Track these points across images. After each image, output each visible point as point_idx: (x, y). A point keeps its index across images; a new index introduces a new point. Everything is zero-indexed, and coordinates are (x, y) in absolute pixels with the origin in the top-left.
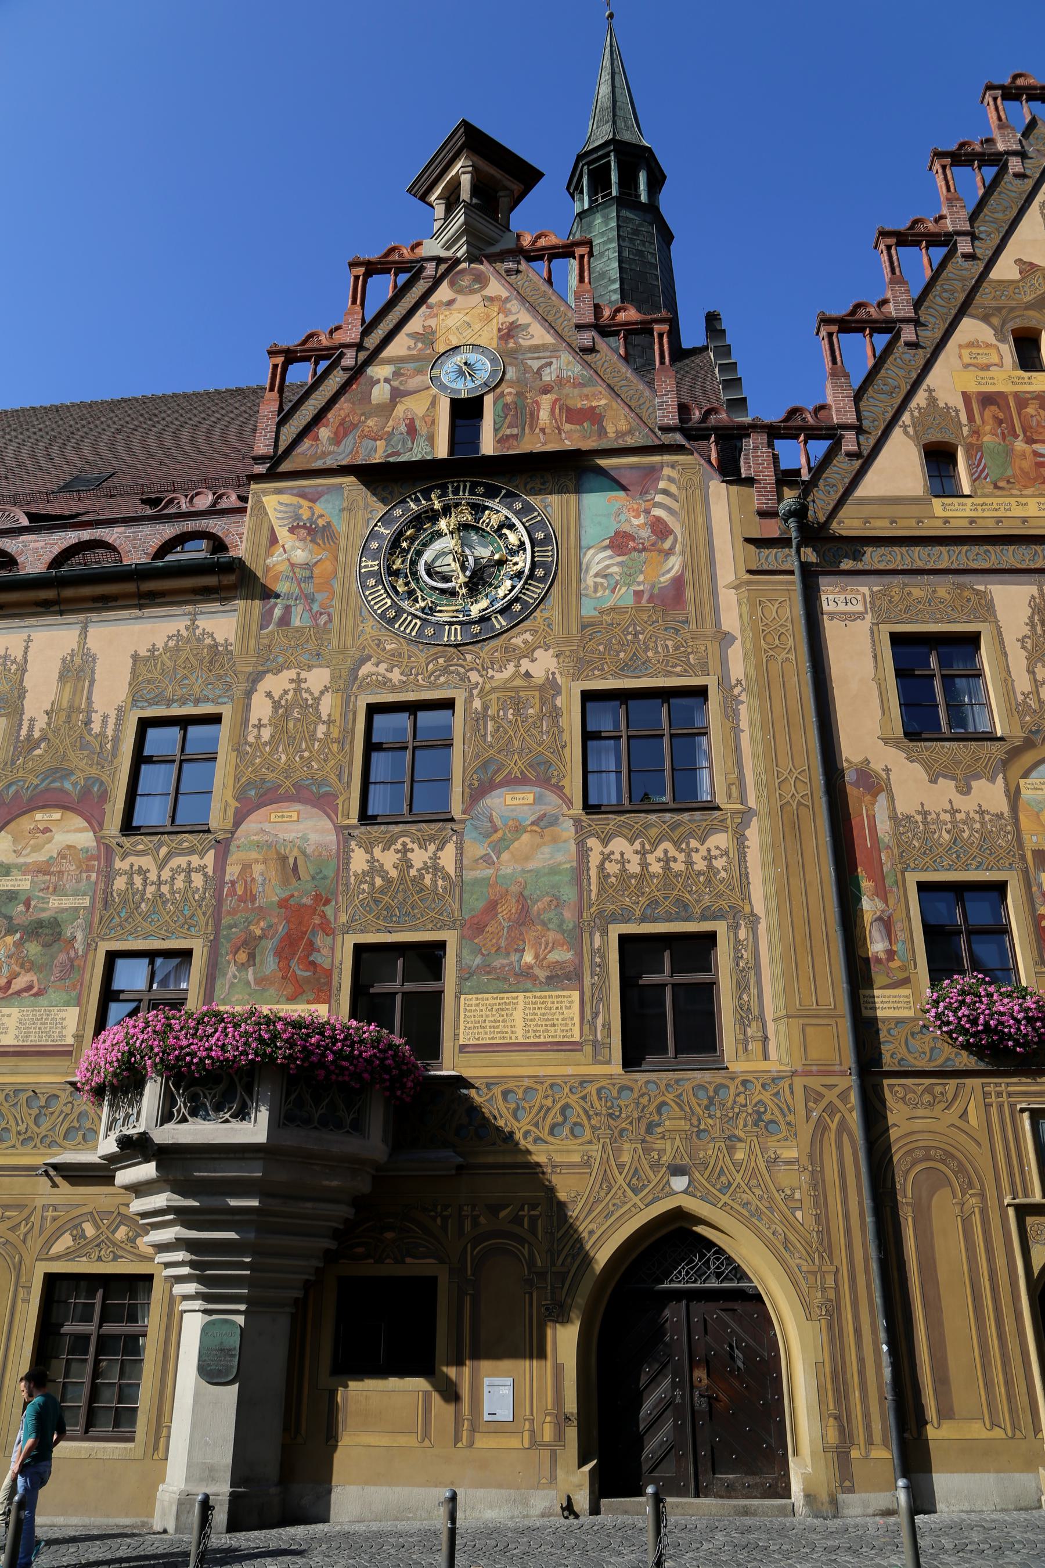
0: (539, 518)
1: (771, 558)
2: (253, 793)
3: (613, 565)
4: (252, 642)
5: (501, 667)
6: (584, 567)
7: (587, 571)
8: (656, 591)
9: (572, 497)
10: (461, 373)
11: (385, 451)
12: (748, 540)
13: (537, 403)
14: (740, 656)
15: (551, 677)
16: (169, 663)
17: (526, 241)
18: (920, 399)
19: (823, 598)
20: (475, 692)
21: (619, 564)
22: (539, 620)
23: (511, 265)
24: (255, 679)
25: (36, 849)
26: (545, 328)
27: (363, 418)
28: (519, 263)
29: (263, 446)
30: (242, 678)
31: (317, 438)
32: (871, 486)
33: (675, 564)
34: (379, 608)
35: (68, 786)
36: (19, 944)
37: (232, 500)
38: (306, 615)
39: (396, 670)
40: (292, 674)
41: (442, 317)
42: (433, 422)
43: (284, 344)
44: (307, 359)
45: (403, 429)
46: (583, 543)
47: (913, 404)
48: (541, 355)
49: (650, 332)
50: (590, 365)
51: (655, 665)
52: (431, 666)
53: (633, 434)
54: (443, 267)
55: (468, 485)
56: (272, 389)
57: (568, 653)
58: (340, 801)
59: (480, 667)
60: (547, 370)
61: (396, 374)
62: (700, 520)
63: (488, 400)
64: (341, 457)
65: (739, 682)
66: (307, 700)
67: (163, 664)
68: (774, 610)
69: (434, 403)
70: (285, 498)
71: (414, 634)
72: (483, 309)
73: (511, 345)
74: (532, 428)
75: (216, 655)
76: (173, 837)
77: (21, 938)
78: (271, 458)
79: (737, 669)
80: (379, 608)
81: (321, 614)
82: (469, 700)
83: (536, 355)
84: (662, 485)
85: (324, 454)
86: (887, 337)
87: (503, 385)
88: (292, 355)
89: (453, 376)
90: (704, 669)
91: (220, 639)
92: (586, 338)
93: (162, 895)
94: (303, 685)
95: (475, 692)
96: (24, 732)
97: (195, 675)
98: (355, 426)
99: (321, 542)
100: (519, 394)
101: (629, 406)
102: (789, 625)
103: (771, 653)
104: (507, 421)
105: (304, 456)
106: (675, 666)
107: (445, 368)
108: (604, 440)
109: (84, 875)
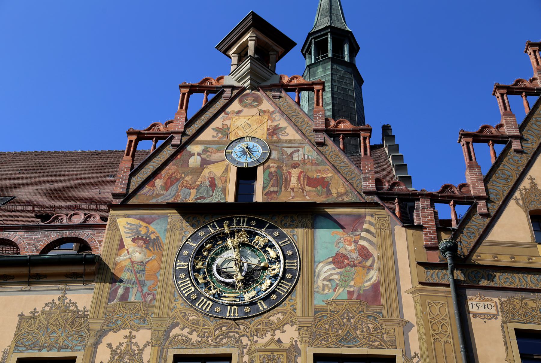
0: (289, 242)
1: (435, 276)
3: (335, 274)
4: (102, 310)
5: (262, 335)
6: (316, 274)
7: (318, 276)
8: (362, 292)
9: (310, 231)
10: (244, 153)
11: (195, 196)
12: (419, 264)
13: (289, 173)
14: (417, 337)
15: (294, 343)
16: (44, 322)
17: (285, 80)
18: (526, 183)
19: (469, 303)
20: (245, 351)
21: (339, 273)
22: (288, 306)
23: (276, 93)
24: (102, 334)
26: (295, 130)
27: (183, 175)
28: (281, 92)
29: (120, 188)
30: (92, 333)
31: (154, 186)
32: (498, 234)
33: (374, 276)
34: (186, 293)
37: (96, 219)
38: (139, 294)
39: (194, 333)
40: (126, 332)
41: (234, 120)
42: (226, 181)
43: (137, 129)
44: (150, 138)
45: (208, 183)
46: (316, 259)
47: (521, 186)
48: (293, 145)
49: (359, 136)
50: (322, 153)
51: (361, 340)
52: (217, 332)
53: (348, 195)
54: (235, 92)
55: (246, 219)
56: (128, 155)
57: (305, 329)
59: (249, 334)
60: (296, 155)
61: (205, 151)
62: (389, 249)
63: (260, 170)
64: (168, 198)
65: (416, 355)
66: (135, 350)
67: (40, 322)
68: (438, 308)
69: (227, 169)
70: (131, 220)
71: (207, 310)
72: (259, 117)
73: (275, 138)
74: (286, 188)
75: (77, 317)
78: (124, 195)
79: (415, 347)
80: (186, 293)
81: (149, 294)
82: (241, 356)
83: (290, 145)
84: (365, 226)
85: (158, 195)
86: (503, 146)
87: (270, 161)
88: (141, 136)
89: (239, 154)
90: (393, 344)
91: (80, 307)
92: (320, 137)
94: (133, 340)
95: (245, 351)
97: (61, 330)
98: (178, 180)
99: (152, 249)
100: (279, 167)
101: (346, 178)
102: (448, 319)
103: (437, 337)
104: (271, 183)
105: (146, 195)
106: (374, 341)
107: (235, 149)
108: (330, 198)
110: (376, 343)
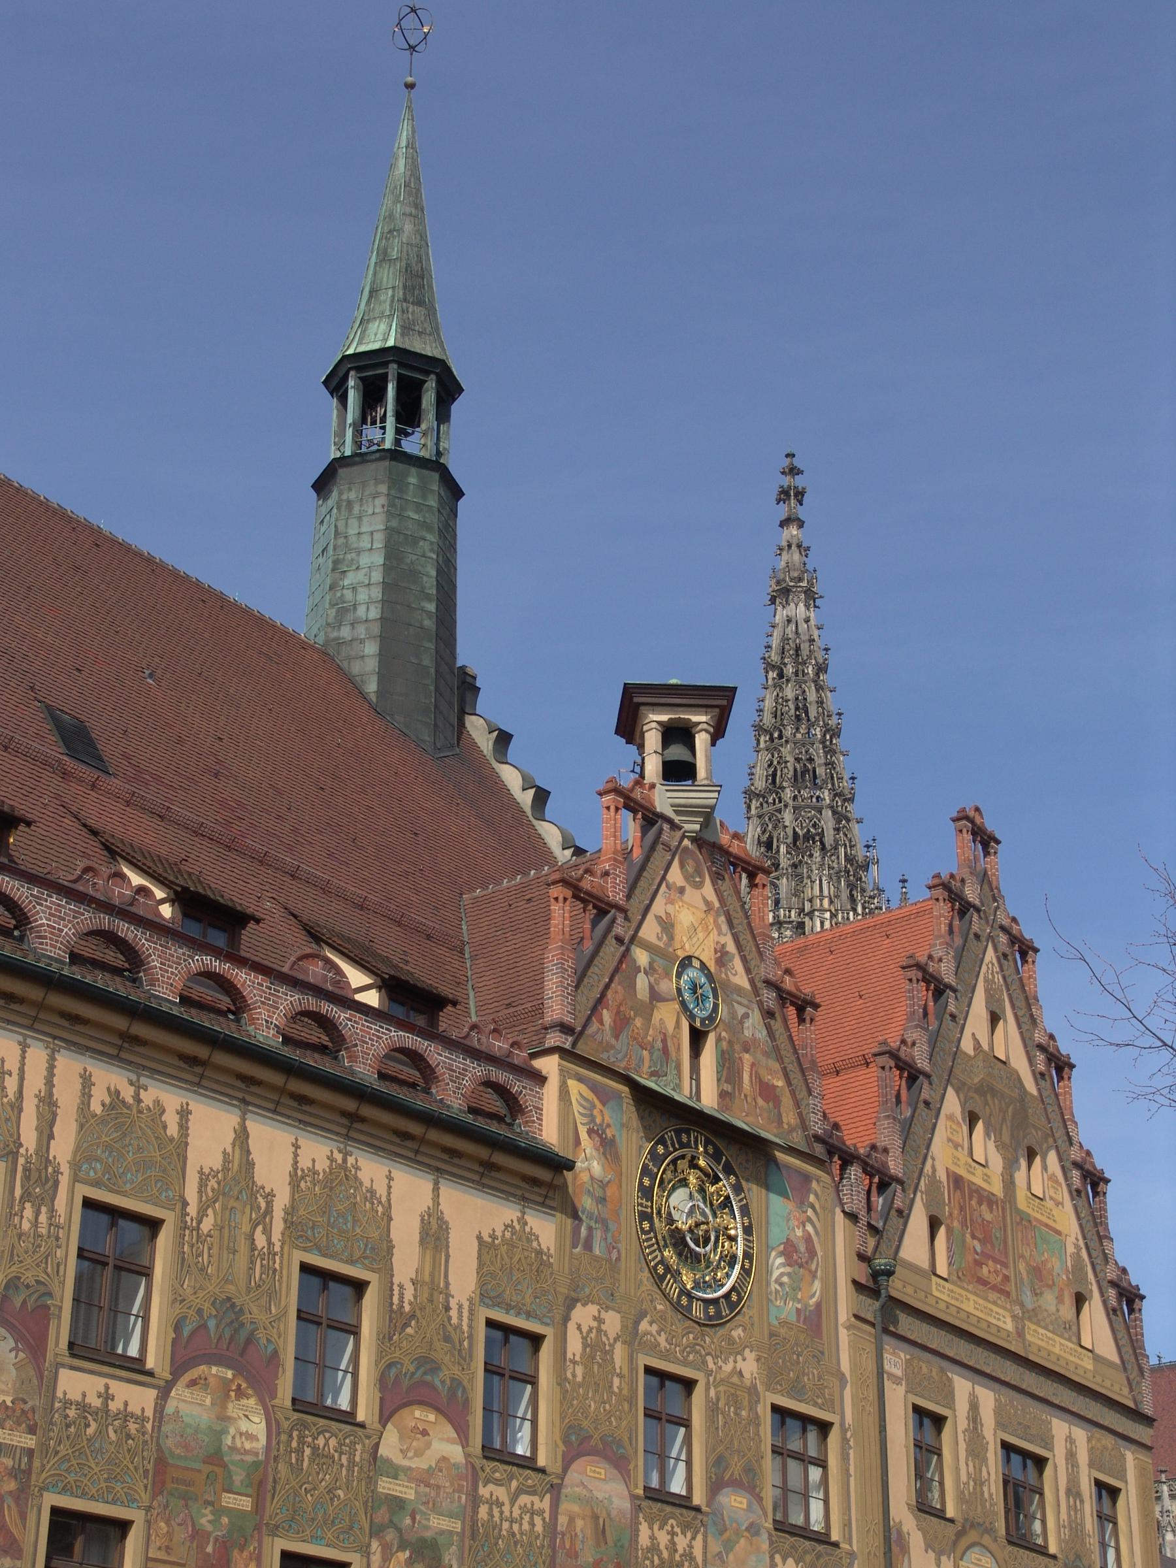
2: (573, 1438)
12: (854, 1282)
20: (711, 1379)
21: (789, 1275)
25: (419, 1453)
30: (561, 1299)
40: (593, 1309)
58: (631, 1467)
76: (521, 1470)
77: (411, 1557)
90: (829, 1405)
91: (544, 1247)
93: (514, 1534)
96: (396, 1300)
109: (457, 1495)
110: (820, 1401)
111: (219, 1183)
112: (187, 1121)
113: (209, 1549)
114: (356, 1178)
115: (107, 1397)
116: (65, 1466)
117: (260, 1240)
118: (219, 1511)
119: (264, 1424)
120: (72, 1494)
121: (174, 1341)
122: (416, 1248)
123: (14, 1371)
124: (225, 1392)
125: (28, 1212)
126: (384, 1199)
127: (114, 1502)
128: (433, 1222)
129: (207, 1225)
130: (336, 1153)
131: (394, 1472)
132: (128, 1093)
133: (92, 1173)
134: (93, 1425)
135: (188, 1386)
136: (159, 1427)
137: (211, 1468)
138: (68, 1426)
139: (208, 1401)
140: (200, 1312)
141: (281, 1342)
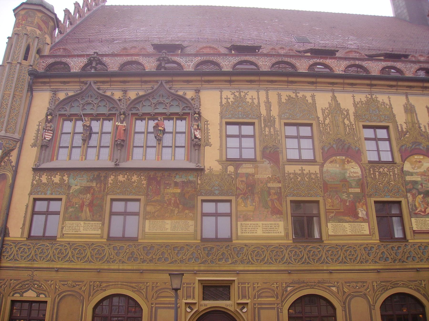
25: (419, 167)
35: (421, 148)
36: (423, 198)
77: (424, 196)
96: (400, 128)
111: (329, 111)
112: (314, 98)
113: (348, 204)
114: (377, 100)
115: (302, 170)
116: (292, 189)
117: (347, 122)
118: (349, 194)
119: (359, 168)
120: (296, 196)
121: (322, 153)
122: (404, 114)
123: (270, 169)
124: (343, 162)
125: (267, 129)
126: (388, 104)
127: (311, 196)
128: (408, 106)
129: (327, 122)
130: (368, 96)
131: (411, 174)
132: (293, 95)
133: (286, 116)
134: (299, 179)
135: (330, 163)
136: (322, 175)
137: (343, 183)
138: (291, 179)
139: (338, 166)
140: (330, 144)
141: (360, 147)
